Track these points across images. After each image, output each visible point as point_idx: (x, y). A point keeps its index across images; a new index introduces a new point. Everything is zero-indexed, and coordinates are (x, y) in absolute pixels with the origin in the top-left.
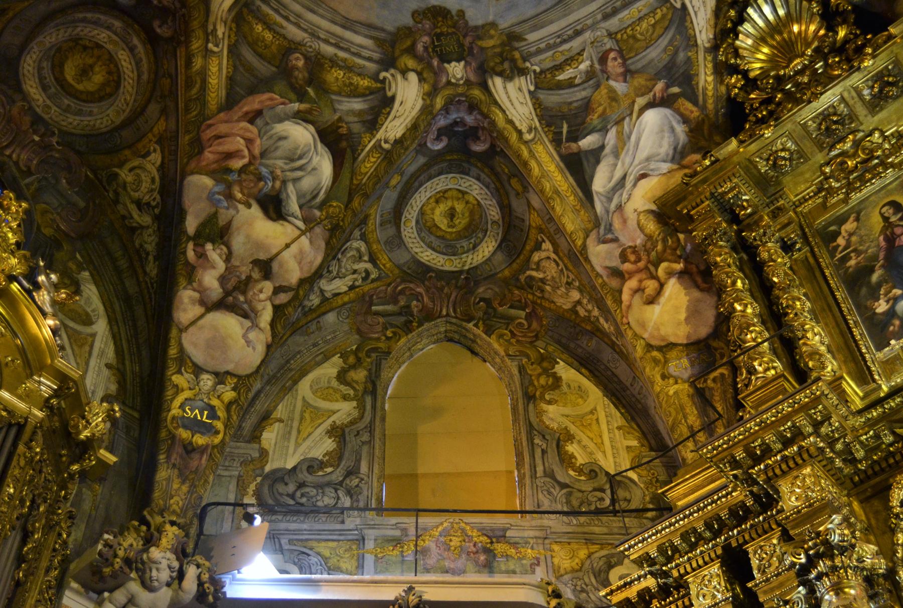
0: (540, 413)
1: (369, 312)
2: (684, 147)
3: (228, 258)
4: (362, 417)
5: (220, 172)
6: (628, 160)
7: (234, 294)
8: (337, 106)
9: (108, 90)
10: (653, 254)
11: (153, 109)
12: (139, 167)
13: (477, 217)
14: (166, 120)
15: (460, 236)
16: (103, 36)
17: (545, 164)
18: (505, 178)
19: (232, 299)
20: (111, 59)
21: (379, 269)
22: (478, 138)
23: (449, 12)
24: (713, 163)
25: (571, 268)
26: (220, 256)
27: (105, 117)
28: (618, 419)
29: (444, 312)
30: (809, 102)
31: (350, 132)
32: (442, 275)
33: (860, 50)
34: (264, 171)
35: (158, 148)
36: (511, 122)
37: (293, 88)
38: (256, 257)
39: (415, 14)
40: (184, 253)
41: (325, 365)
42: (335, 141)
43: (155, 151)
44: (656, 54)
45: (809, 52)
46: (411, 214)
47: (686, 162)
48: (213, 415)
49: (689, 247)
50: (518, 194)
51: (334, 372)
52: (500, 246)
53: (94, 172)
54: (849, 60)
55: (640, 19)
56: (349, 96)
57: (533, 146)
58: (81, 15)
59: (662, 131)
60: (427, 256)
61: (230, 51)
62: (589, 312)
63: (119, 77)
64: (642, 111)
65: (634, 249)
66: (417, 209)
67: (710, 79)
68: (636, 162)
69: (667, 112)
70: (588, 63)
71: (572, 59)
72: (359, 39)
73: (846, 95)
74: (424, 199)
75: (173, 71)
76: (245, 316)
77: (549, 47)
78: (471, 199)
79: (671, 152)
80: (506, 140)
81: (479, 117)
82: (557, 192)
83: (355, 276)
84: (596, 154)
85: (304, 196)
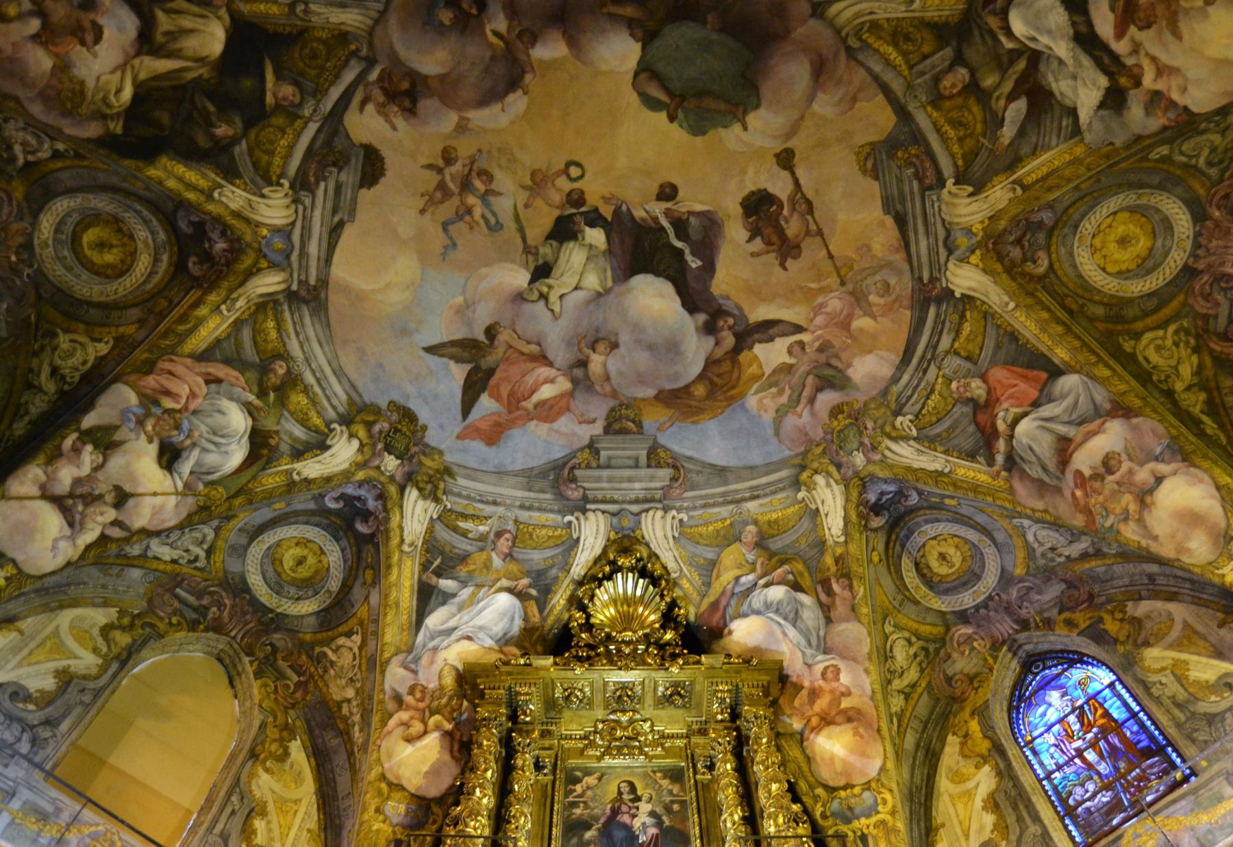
0: (252, 775)
1: (171, 591)
2: (512, 638)
3: (97, 469)
4: (97, 677)
5: (149, 400)
6: (466, 618)
7: (77, 500)
8: (283, 421)
9: (109, 272)
10: (436, 703)
11: (134, 313)
12: (81, 344)
13: (319, 578)
14: (140, 328)
16: (142, 233)
17: (404, 578)
18: (364, 564)
19: (68, 505)
20: (133, 254)
21: (209, 562)
22: (367, 522)
23: (417, 420)
24: (525, 665)
25: (364, 668)
26: (92, 462)
27: (88, 288)
29: (233, 634)
30: (620, 669)
31: (277, 447)
32: (255, 603)
33: (674, 657)
34: (186, 425)
35: (111, 343)
36: (401, 529)
37: (260, 384)
38: (121, 484)
40: (64, 438)
41: (100, 610)
43: (107, 343)
44: (538, 557)
45: (640, 633)
46: (269, 539)
47: (506, 649)
49: (465, 716)
50: (365, 583)
51: (103, 621)
52: (319, 612)
54: (663, 658)
55: (544, 526)
56: (297, 421)
57: (404, 558)
58: (138, 207)
59: (504, 615)
60: (255, 581)
61: (235, 322)
62: (351, 714)
63: (127, 271)
64: (501, 590)
65: (424, 690)
66: (277, 538)
67: (562, 602)
68: (471, 624)
70: (487, 528)
71: (478, 517)
72: (338, 388)
73: (647, 681)
74: (288, 535)
75: (176, 300)
77: (468, 498)
78: (325, 561)
79: (500, 635)
80: (388, 539)
81: (380, 507)
82: (397, 605)
83: (185, 554)
84: (447, 597)
85: (201, 466)
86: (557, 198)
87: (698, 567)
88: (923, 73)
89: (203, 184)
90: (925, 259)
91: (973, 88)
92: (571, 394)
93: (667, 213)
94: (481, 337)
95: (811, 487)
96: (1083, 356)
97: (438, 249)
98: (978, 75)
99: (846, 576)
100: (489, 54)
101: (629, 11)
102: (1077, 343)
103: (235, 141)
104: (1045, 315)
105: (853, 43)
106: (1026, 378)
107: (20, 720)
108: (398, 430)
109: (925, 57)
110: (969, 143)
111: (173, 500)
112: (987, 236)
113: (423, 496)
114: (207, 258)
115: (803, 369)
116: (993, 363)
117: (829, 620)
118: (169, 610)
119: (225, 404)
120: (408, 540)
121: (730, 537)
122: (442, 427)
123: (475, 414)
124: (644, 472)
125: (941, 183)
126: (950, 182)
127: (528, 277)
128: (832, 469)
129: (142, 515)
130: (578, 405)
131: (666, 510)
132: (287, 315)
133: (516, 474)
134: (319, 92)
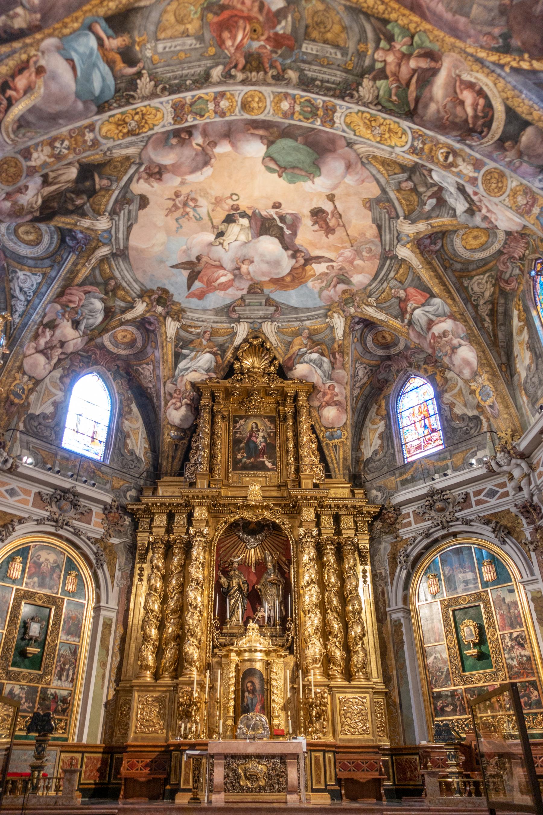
0: (123, 423)
3: (52, 336)
11: (47, 262)
15: (122, 343)
20: (41, 235)
27: (24, 250)
28: (145, 435)
32: (108, 351)
34: (80, 312)
37: (105, 289)
39: (158, 288)
42: (109, 312)
44: (220, 340)
48: (23, 392)
51: (59, 375)
53: (8, 265)
60: (107, 344)
69: (213, 357)
72: (136, 286)
76: (48, 359)
80: (161, 336)
84: (185, 356)
86: (227, 207)
87: (284, 343)
88: (394, 179)
89: (73, 221)
90: (388, 242)
91: (414, 190)
92: (233, 280)
93: (277, 213)
94: (195, 260)
95: (332, 317)
96: (444, 294)
97: (174, 228)
98: (418, 187)
99: (342, 353)
100: (194, 153)
101: (261, 132)
102: (442, 288)
103: (84, 204)
104: (432, 274)
105: (364, 160)
106: (421, 295)
107: (49, 427)
108: (163, 297)
109: (395, 174)
110: (411, 207)
111: (80, 339)
112: (414, 239)
113: (173, 319)
114: (74, 238)
115: (332, 275)
116: (410, 286)
117: (333, 368)
118: (78, 361)
119: (93, 300)
120: (169, 336)
121: (297, 333)
122: (179, 294)
123: (193, 288)
124: (263, 308)
125: (398, 217)
126: (401, 218)
127: (214, 237)
128: (341, 312)
129: (70, 348)
130: (237, 284)
131: (272, 322)
132: (113, 262)
133: (211, 310)
134: (119, 179)
